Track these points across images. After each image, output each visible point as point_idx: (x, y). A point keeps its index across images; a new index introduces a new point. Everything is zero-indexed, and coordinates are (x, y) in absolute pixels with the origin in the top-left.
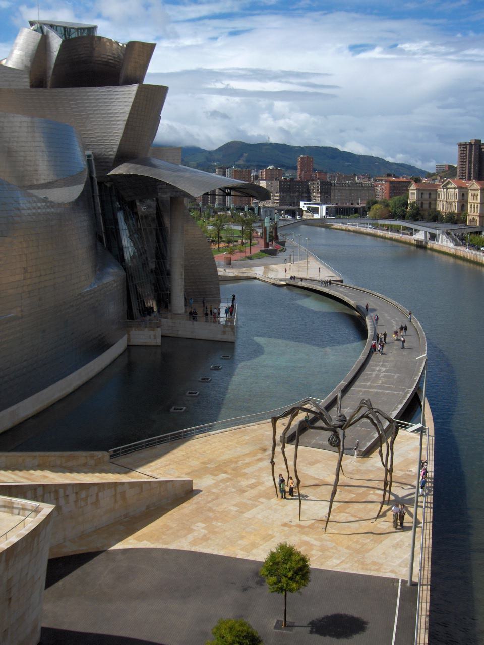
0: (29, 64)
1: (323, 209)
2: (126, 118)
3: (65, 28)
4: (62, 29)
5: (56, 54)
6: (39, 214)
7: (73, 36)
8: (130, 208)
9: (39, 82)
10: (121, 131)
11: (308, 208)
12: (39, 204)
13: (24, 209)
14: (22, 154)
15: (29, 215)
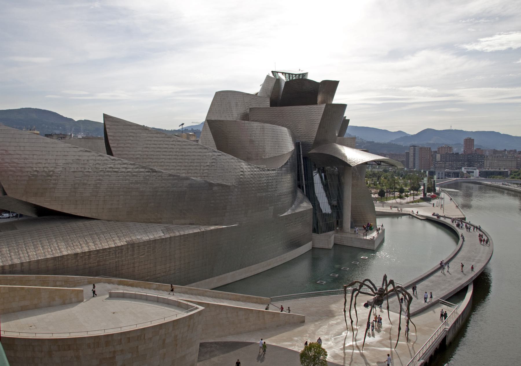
0: (270, 94)
1: (477, 172)
2: (319, 122)
3: (289, 74)
4: (287, 75)
5: (283, 88)
6: (255, 174)
7: (294, 78)
8: (322, 170)
9: (274, 103)
10: (317, 129)
11: (467, 172)
12: (255, 169)
13: (246, 172)
14: (257, 142)
15: (249, 175)
